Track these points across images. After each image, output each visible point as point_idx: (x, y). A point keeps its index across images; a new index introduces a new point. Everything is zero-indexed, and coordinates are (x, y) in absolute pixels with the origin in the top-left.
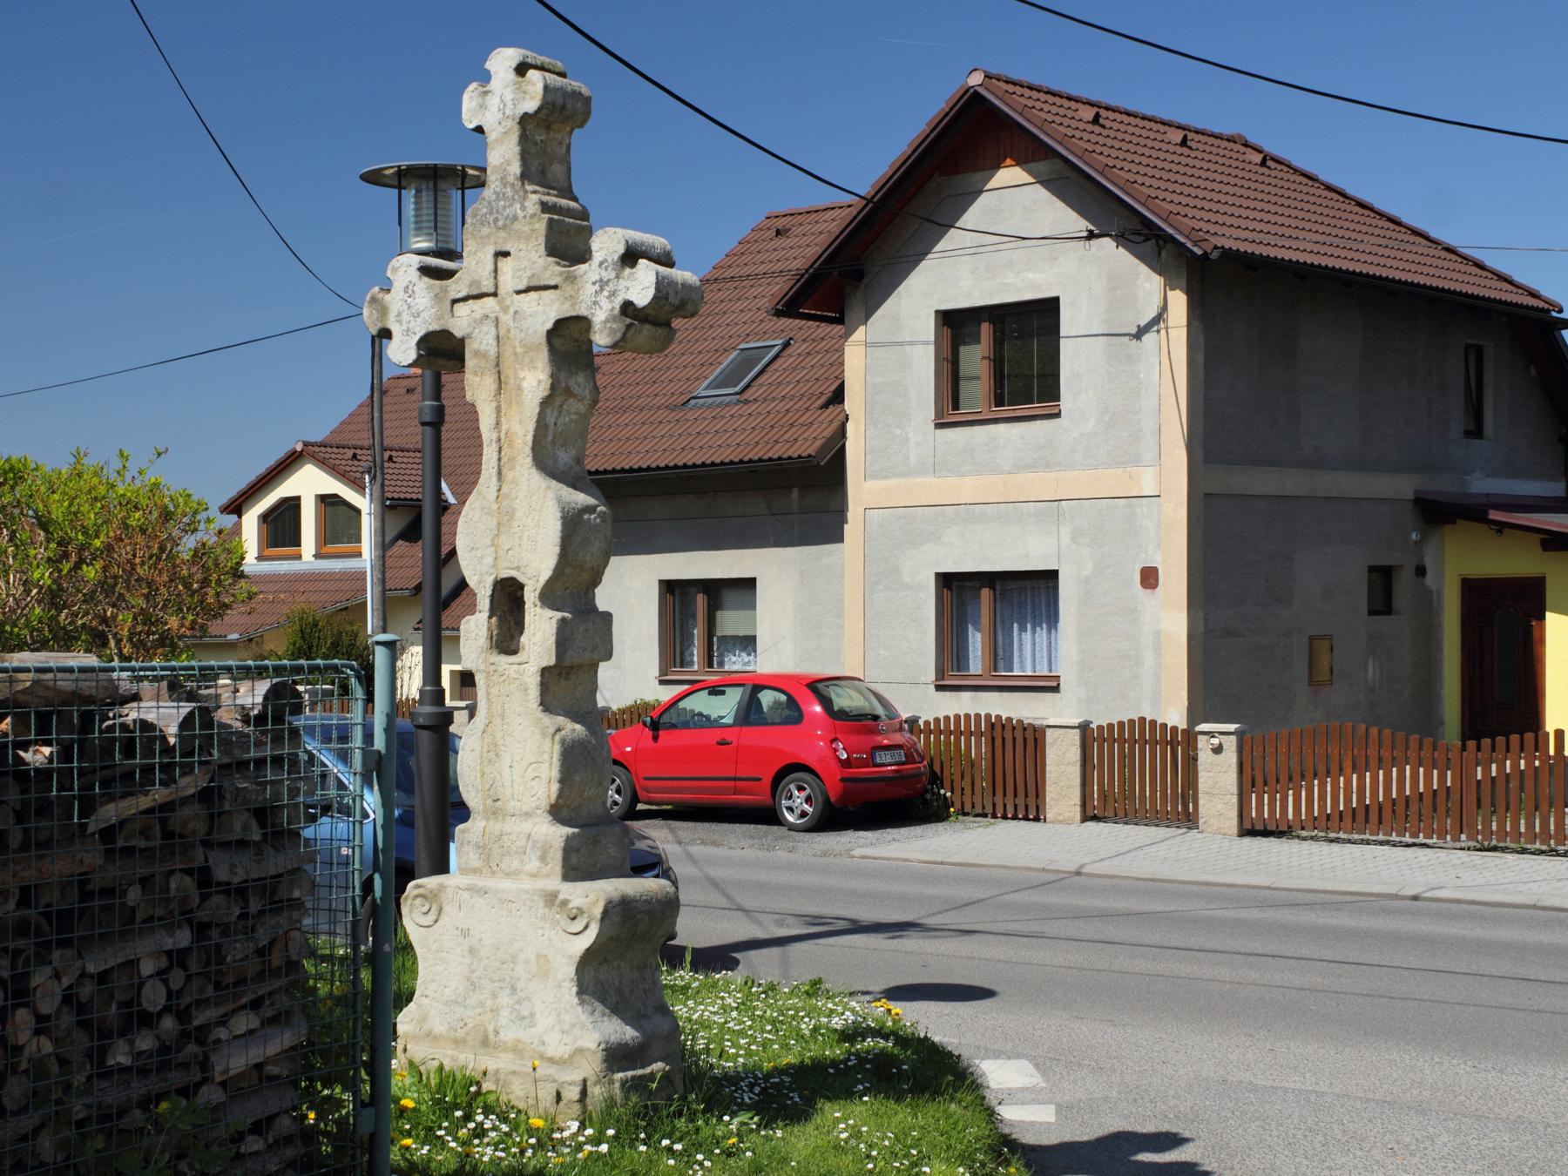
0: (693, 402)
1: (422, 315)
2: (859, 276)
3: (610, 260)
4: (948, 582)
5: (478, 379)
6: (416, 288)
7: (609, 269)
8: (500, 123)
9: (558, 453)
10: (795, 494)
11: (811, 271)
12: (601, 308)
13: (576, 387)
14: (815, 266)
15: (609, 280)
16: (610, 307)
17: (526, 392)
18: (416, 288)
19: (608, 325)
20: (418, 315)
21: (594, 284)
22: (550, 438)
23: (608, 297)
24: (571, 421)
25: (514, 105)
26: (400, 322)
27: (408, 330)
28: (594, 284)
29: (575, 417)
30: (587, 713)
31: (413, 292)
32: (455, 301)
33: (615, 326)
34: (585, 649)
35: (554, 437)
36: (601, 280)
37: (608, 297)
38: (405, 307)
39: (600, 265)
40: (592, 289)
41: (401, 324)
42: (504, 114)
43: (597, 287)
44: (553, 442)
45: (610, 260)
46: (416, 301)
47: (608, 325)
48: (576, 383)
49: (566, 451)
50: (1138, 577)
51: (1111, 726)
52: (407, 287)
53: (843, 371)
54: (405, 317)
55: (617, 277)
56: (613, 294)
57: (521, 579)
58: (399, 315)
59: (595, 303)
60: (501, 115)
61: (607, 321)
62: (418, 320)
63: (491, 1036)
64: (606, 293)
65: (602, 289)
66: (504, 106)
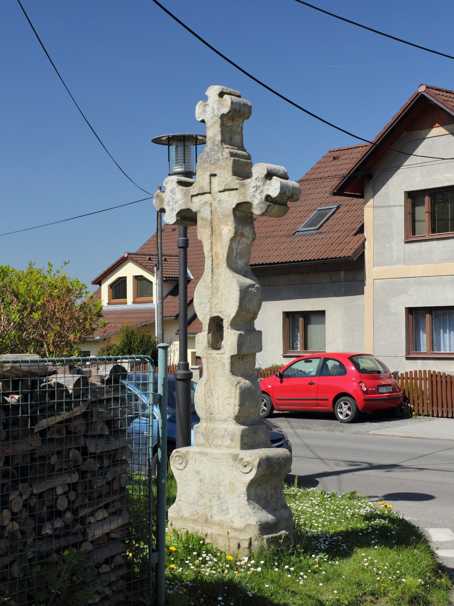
0: (297, 233)
1: (178, 202)
2: (370, 177)
3: (260, 177)
4: (410, 311)
5: (203, 230)
6: (176, 191)
7: (260, 181)
8: (212, 118)
9: (238, 261)
10: (342, 273)
11: (349, 175)
12: (256, 198)
13: (246, 233)
14: (351, 173)
15: (260, 186)
17: (224, 235)
18: (176, 191)
19: (260, 206)
20: (177, 202)
21: (253, 187)
22: (234, 255)
23: (259, 193)
24: (244, 247)
25: (218, 110)
26: (169, 205)
27: (172, 209)
28: (253, 187)
29: (245, 246)
31: (175, 192)
32: (193, 196)
33: (262, 206)
34: (250, 347)
35: (236, 254)
36: (256, 186)
37: (259, 193)
38: (171, 199)
39: (256, 180)
40: (252, 190)
42: (214, 114)
43: (255, 189)
44: (236, 257)
45: (260, 177)
46: (176, 196)
47: (260, 206)
48: (246, 231)
49: (241, 261)
52: (172, 190)
53: (363, 219)
54: (171, 203)
55: (263, 184)
56: (262, 192)
57: (222, 317)
58: (168, 202)
59: (254, 196)
60: (212, 115)
61: (259, 204)
62: (177, 204)
63: (209, 518)
64: (258, 192)
65: (257, 190)
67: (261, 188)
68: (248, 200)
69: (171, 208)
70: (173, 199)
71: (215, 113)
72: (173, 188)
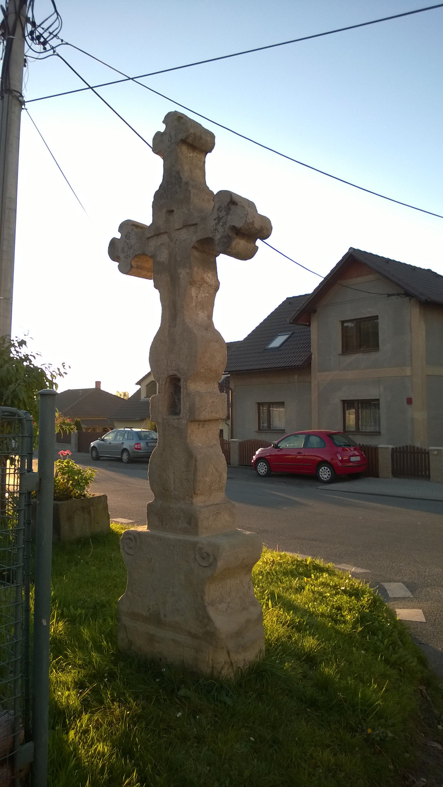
2: (315, 311)
3: (223, 206)
4: (344, 402)
5: (159, 276)
6: (130, 235)
7: (223, 211)
10: (296, 377)
11: (301, 309)
12: (218, 232)
13: (207, 278)
14: (303, 308)
15: (223, 217)
16: (223, 230)
17: (181, 280)
18: (130, 235)
19: (222, 240)
20: (132, 248)
21: (215, 220)
22: (194, 304)
23: (222, 226)
24: (205, 297)
25: (176, 137)
26: (123, 252)
27: (127, 255)
28: (215, 220)
29: (207, 295)
30: (214, 445)
31: (129, 237)
32: (148, 238)
33: (226, 240)
34: (212, 412)
35: (196, 304)
36: (218, 217)
37: (222, 226)
38: (126, 244)
39: (218, 210)
40: (213, 223)
41: (124, 253)
42: (171, 142)
43: (216, 221)
45: (223, 206)
47: (222, 240)
49: (203, 312)
50: (405, 401)
51: (403, 447)
53: (310, 340)
54: (126, 249)
55: (227, 214)
56: (225, 223)
57: (179, 375)
58: (123, 249)
59: (215, 230)
61: (222, 238)
62: (131, 250)
63: (162, 616)
64: (221, 224)
65: (219, 222)
66: (171, 138)
67: (223, 219)
68: (211, 236)
69: (125, 255)
70: (128, 244)
71: (172, 141)
72: (128, 232)
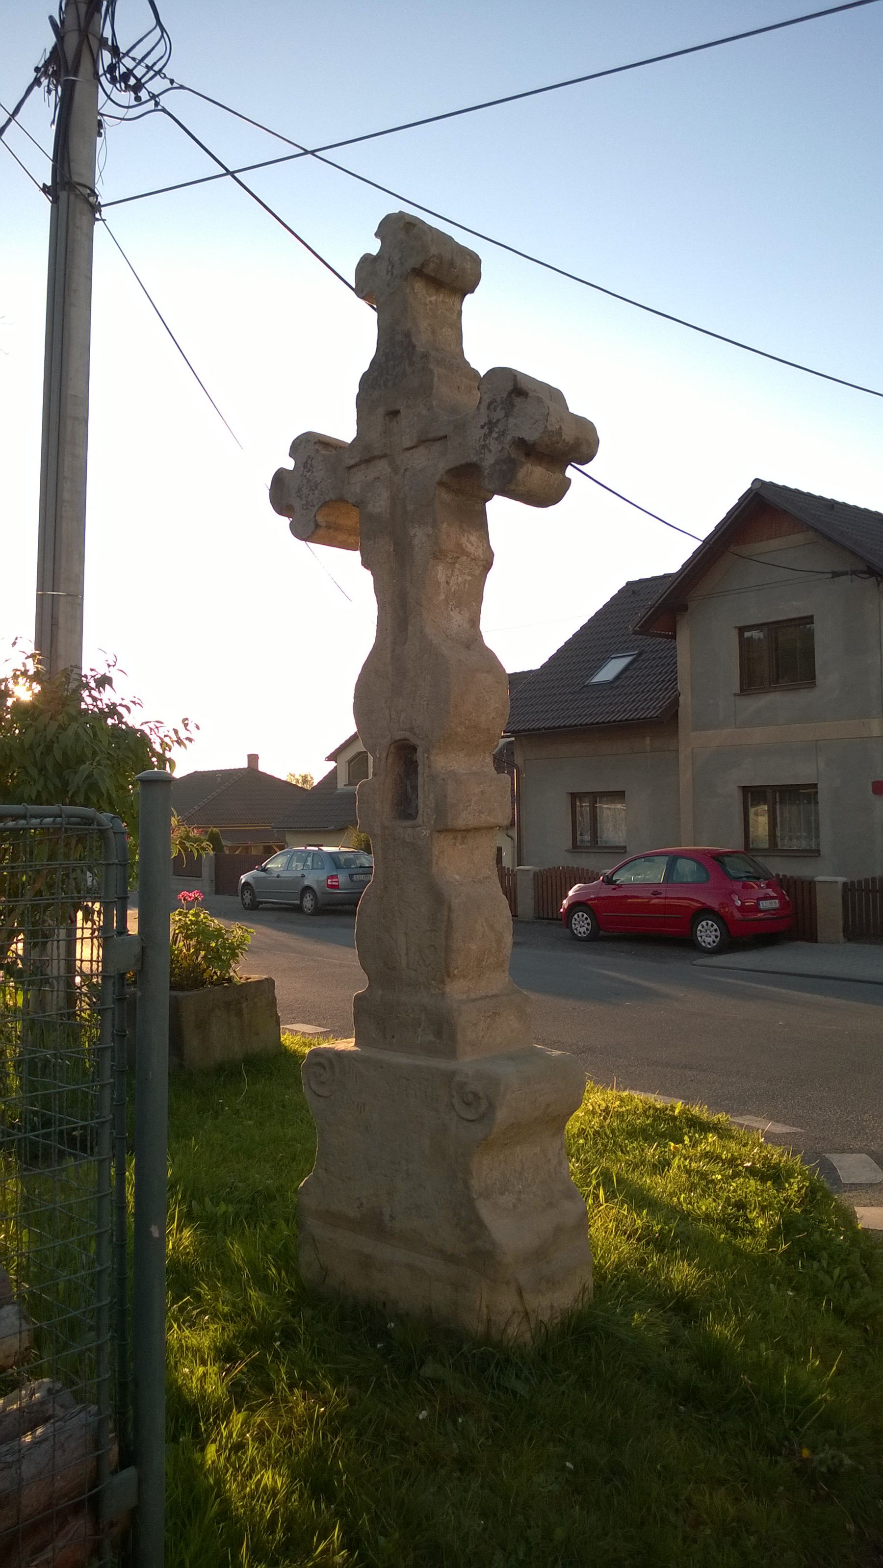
0: (585, 689)
1: (319, 487)
2: (685, 608)
3: (499, 400)
4: (745, 789)
7: (498, 409)
8: (389, 285)
9: (452, 613)
10: (648, 741)
12: (490, 451)
13: (469, 545)
15: (498, 421)
16: (500, 448)
19: (498, 467)
20: (316, 488)
22: (443, 597)
25: (402, 263)
26: (300, 497)
28: (482, 427)
29: (469, 578)
30: (486, 878)
31: (311, 465)
32: (350, 468)
33: (505, 467)
34: (481, 812)
36: (490, 422)
38: (305, 481)
39: (488, 408)
41: (302, 499)
42: (392, 275)
44: (446, 601)
45: (499, 400)
46: (315, 474)
47: (498, 467)
48: (468, 540)
50: (870, 788)
51: (867, 880)
52: (306, 462)
54: (305, 491)
56: (503, 433)
57: (414, 741)
58: (299, 490)
59: (484, 447)
60: (389, 277)
61: (497, 463)
62: (316, 492)
63: (387, 1218)
64: (494, 435)
65: (491, 432)
66: (393, 267)
67: (500, 425)
68: (474, 459)
69: (304, 502)
70: (309, 481)
71: (395, 273)
72: (309, 457)
